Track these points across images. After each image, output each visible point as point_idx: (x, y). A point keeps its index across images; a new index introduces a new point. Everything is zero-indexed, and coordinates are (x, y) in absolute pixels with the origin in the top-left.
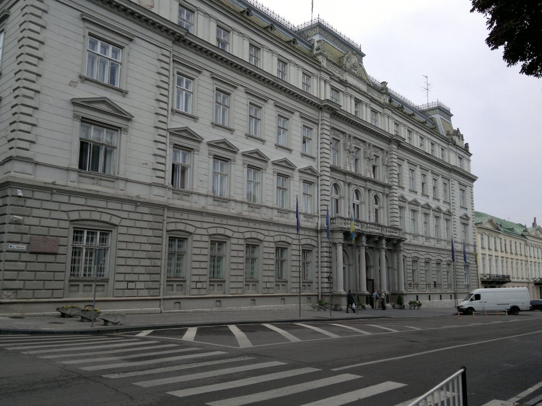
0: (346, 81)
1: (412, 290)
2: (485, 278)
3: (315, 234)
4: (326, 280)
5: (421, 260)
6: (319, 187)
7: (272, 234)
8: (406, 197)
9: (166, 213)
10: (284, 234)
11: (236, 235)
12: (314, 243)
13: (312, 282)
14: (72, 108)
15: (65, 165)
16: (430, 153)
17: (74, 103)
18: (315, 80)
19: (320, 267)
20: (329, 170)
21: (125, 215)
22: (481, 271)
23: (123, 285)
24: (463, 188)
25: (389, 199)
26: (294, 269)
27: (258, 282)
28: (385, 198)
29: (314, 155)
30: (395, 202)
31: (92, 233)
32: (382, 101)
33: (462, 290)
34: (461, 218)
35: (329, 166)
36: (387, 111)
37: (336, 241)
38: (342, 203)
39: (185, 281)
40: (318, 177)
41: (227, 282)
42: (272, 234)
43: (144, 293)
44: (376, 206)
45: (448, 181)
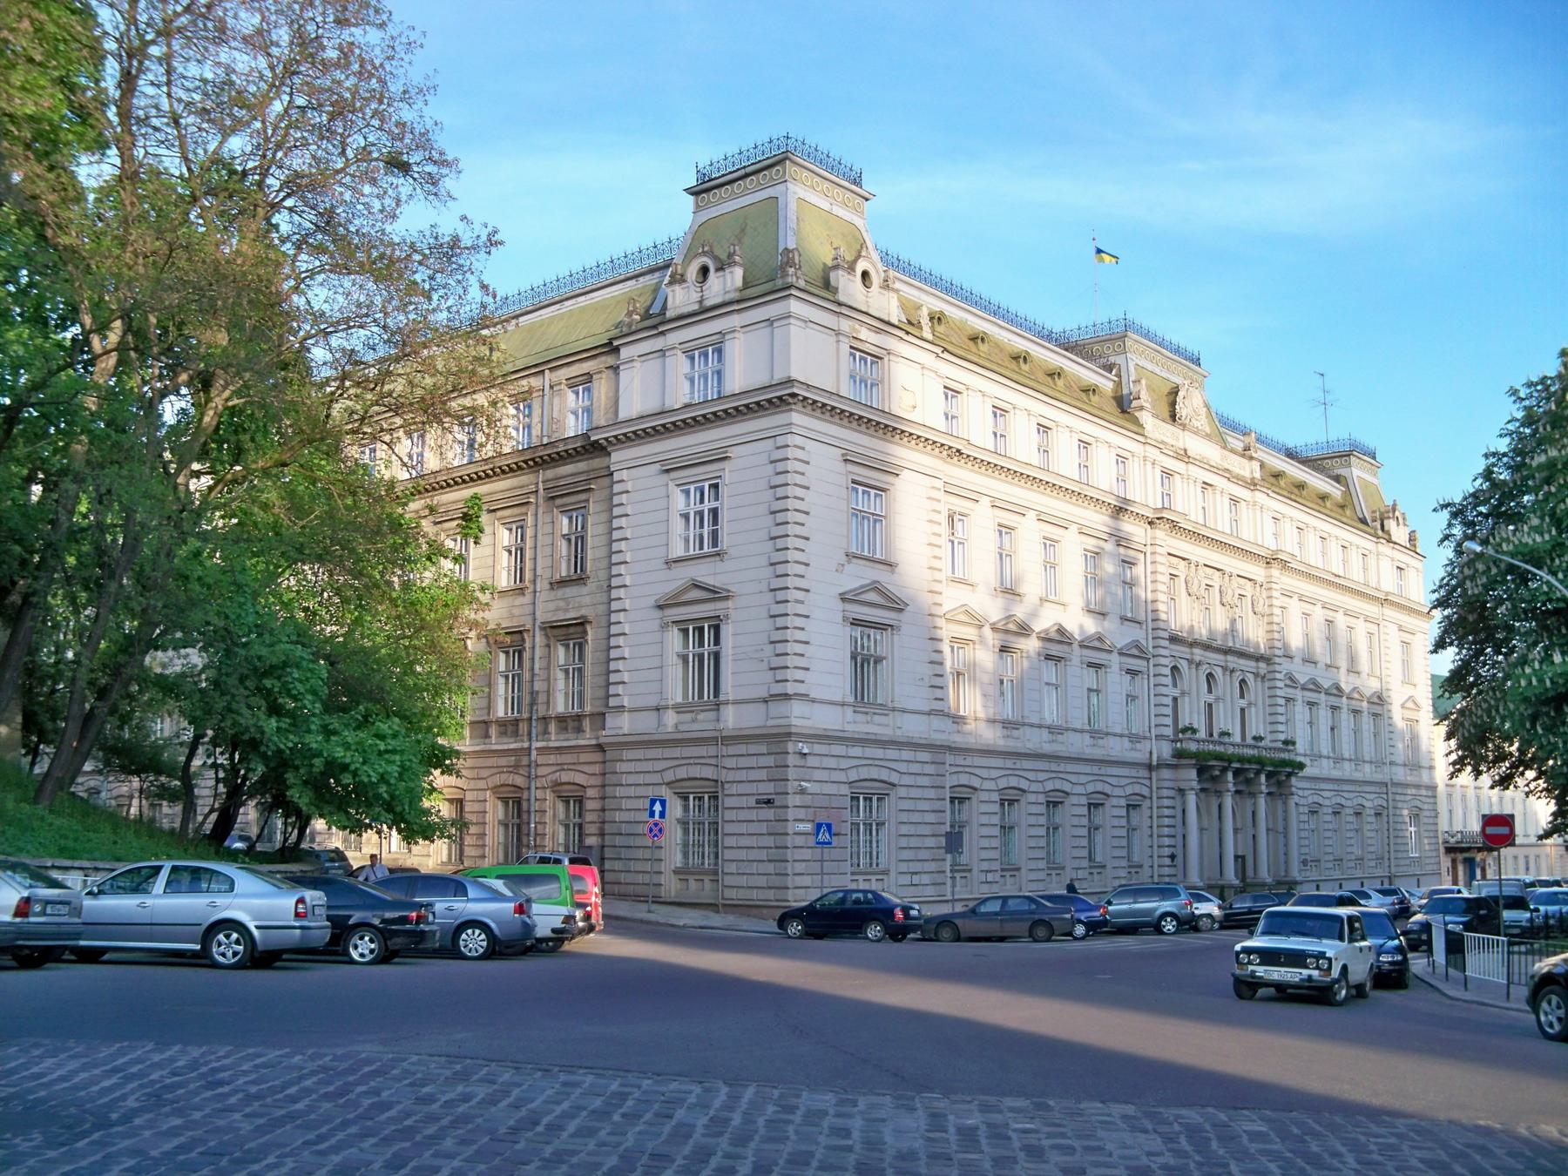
0: (1185, 450)
1: (1308, 874)
2: (1452, 840)
3: (1145, 773)
4: (1167, 861)
5: (1325, 810)
6: (1152, 679)
7: (1083, 779)
8: (1297, 676)
9: (949, 759)
10: (1099, 778)
11: (1034, 787)
12: (1145, 792)
13: (1141, 866)
14: (840, 606)
15: (838, 698)
16: (1342, 574)
17: (844, 598)
18: (1136, 465)
19: (1155, 836)
20: (1166, 643)
21: (903, 767)
22: (1443, 825)
23: (906, 880)
24: (1407, 637)
25: (1267, 684)
26: (1116, 842)
27: (1063, 868)
28: (1259, 683)
29: (1142, 617)
30: (1279, 692)
31: (868, 799)
32: (1247, 474)
33: (1405, 869)
34: (1403, 706)
35: (1166, 635)
36: (1260, 497)
37: (1183, 785)
38: (1185, 706)
39: (970, 871)
40: (1148, 660)
41: (1023, 871)
42: (1083, 779)
43: (930, 891)
44: (1242, 701)
45: (1376, 627)
